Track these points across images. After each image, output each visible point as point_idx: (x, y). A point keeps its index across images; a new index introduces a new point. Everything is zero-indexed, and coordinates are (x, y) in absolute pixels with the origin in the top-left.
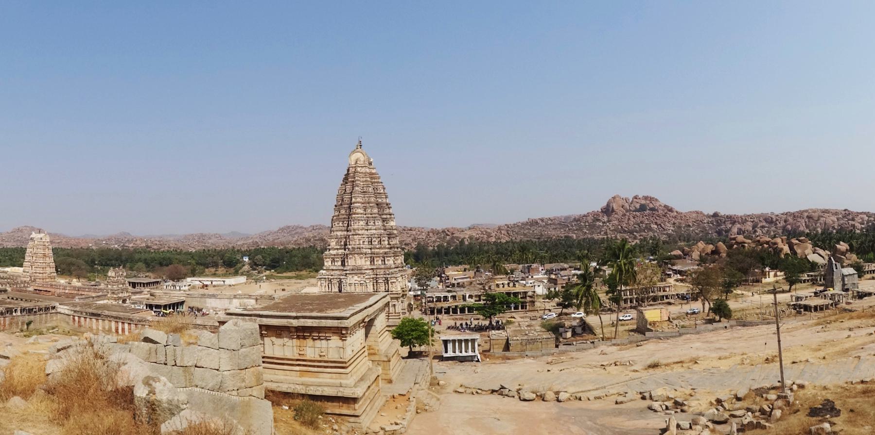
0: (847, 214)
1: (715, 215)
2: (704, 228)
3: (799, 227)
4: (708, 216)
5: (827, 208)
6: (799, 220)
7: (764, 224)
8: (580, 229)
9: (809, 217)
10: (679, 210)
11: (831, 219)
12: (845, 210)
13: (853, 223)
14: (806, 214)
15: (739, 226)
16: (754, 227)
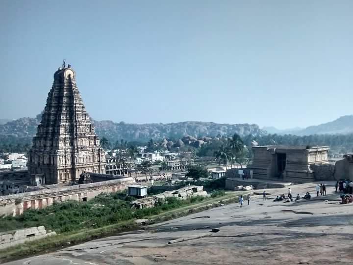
0: (213, 126)
1: (122, 124)
2: (114, 132)
3: (183, 133)
4: (118, 125)
5: (199, 121)
6: (182, 128)
7: (157, 130)
8: (20, 130)
9: (189, 127)
10: (96, 120)
11: (203, 129)
12: (211, 122)
13: (219, 131)
14: (186, 125)
15: (139, 131)
16: (151, 131)
